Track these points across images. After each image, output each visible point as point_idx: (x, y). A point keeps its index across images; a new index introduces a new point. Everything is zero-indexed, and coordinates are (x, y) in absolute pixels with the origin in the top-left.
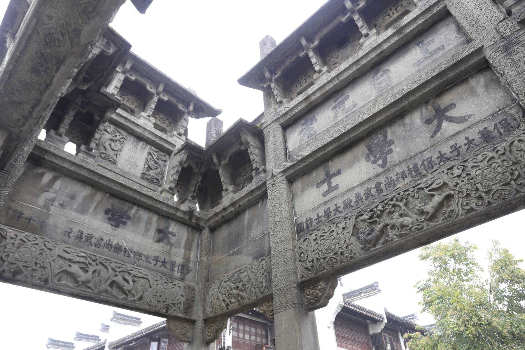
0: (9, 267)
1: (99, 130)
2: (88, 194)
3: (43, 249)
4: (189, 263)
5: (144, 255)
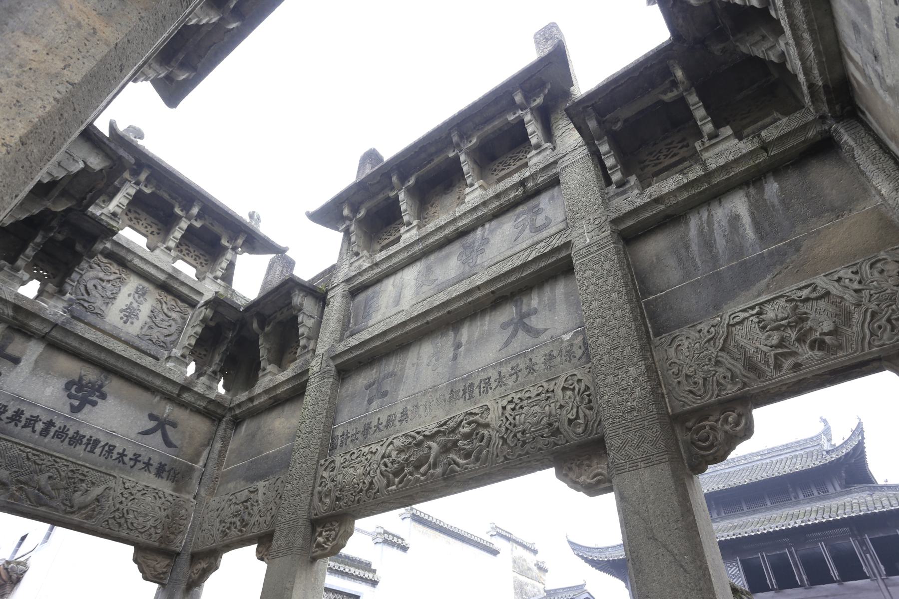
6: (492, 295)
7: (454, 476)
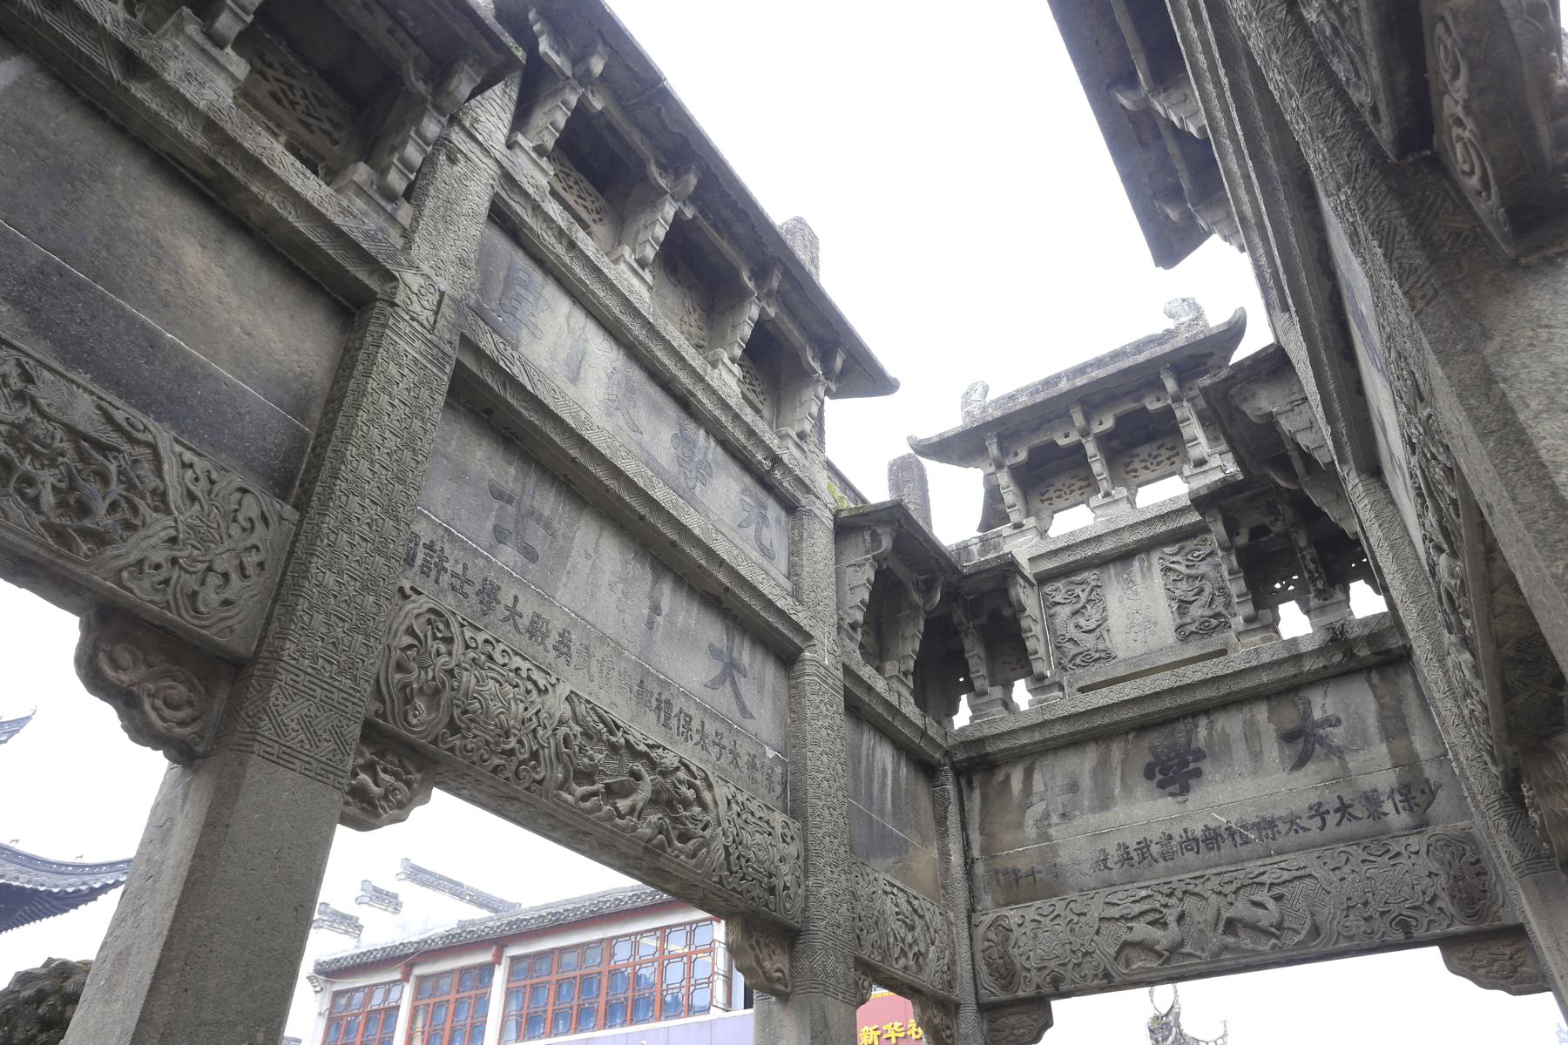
1: (1026, 632)
3: (1072, 920)
4: (1421, 771)
5: (1280, 818)
6: (722, 590)
7: (660, 855)
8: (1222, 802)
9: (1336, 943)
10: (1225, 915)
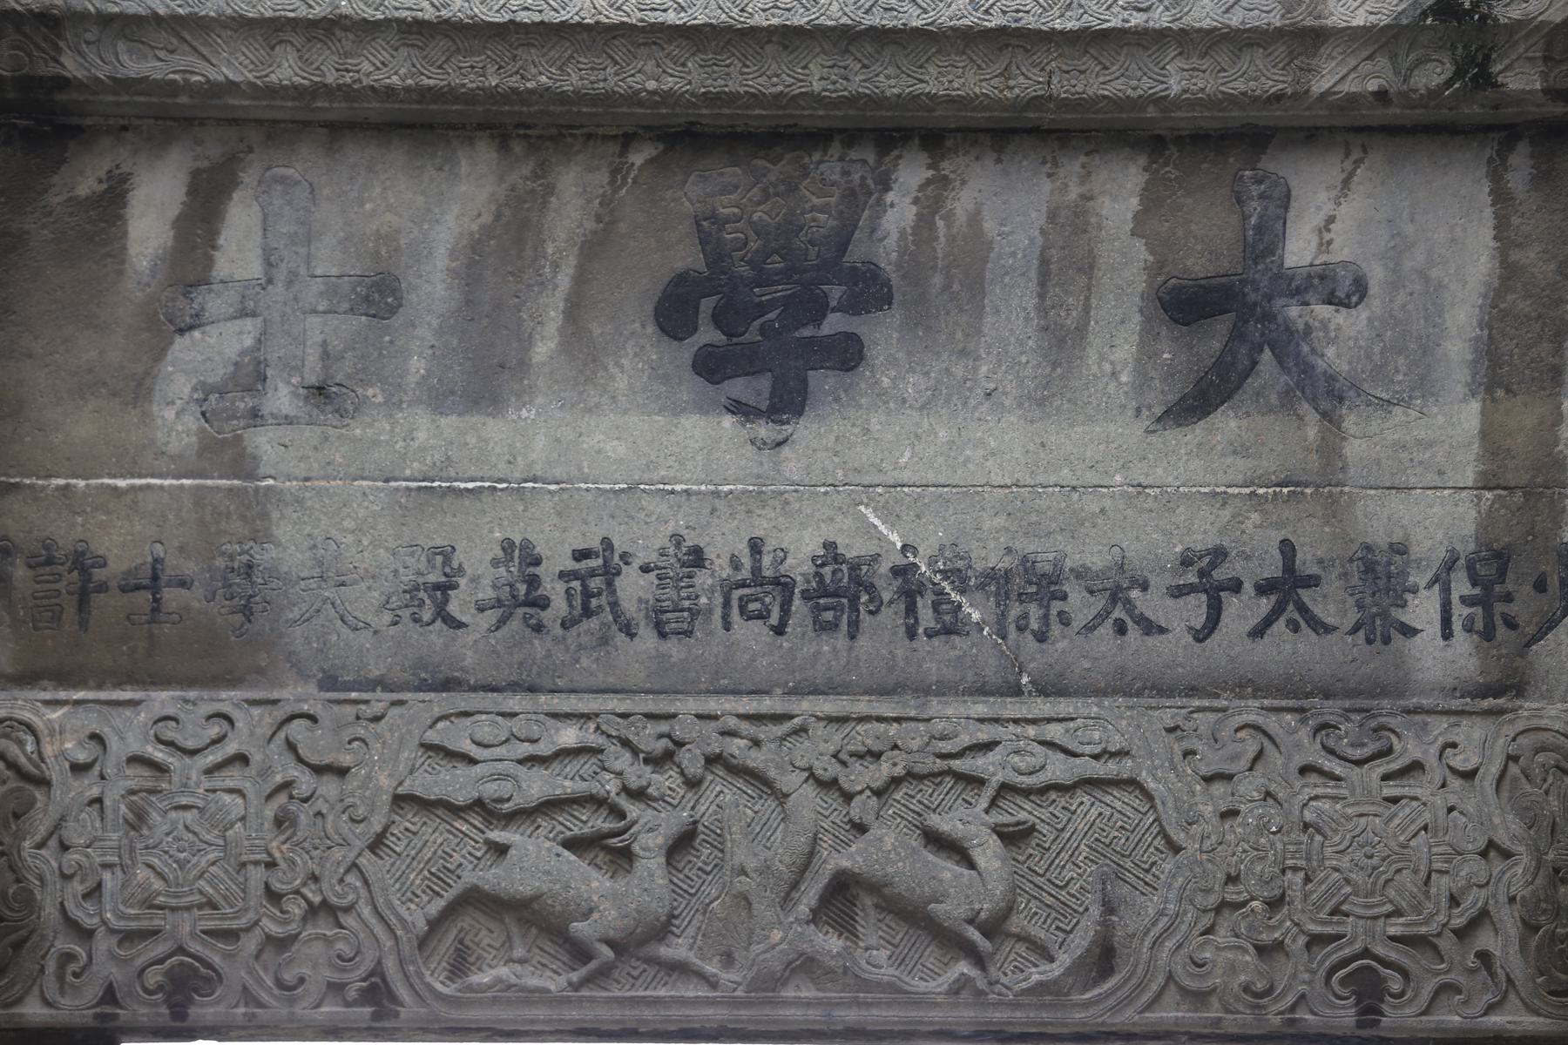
0: (124, 962)
2: (487, 218)
3: (287, 785)
5: (1080, 574)
8: (906, 476)
9: (1149, 1007)
10: (835, 860)
